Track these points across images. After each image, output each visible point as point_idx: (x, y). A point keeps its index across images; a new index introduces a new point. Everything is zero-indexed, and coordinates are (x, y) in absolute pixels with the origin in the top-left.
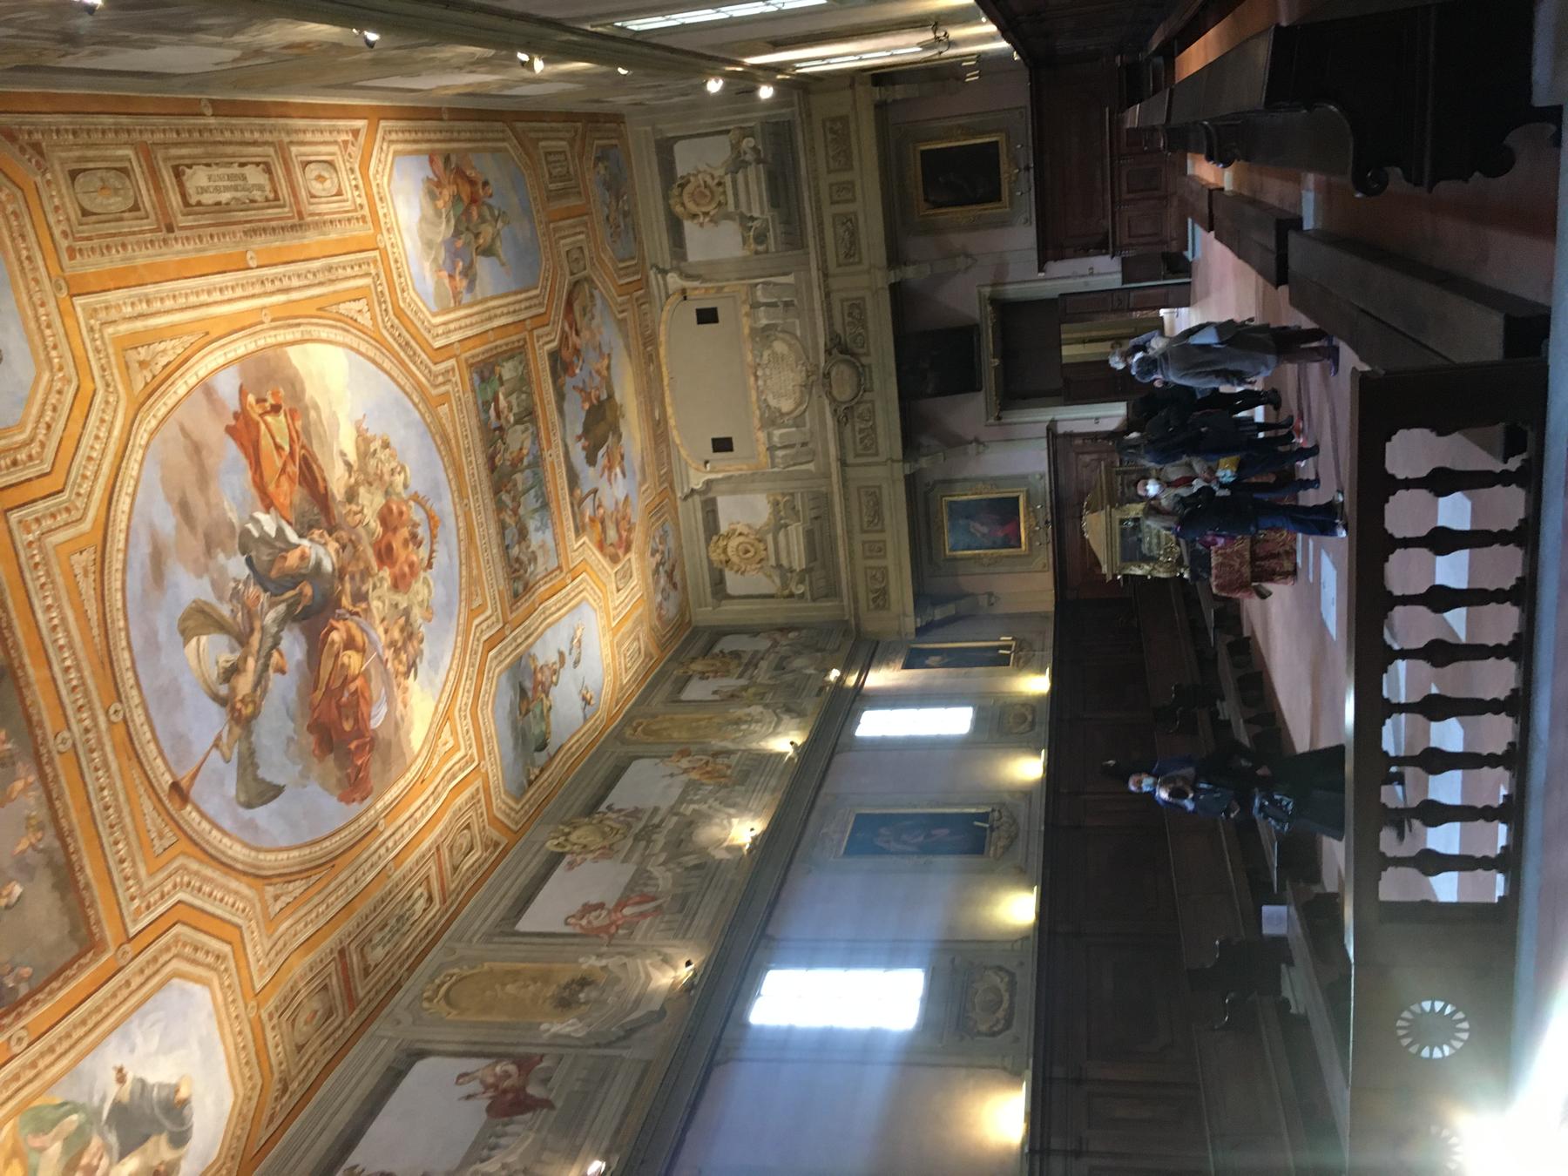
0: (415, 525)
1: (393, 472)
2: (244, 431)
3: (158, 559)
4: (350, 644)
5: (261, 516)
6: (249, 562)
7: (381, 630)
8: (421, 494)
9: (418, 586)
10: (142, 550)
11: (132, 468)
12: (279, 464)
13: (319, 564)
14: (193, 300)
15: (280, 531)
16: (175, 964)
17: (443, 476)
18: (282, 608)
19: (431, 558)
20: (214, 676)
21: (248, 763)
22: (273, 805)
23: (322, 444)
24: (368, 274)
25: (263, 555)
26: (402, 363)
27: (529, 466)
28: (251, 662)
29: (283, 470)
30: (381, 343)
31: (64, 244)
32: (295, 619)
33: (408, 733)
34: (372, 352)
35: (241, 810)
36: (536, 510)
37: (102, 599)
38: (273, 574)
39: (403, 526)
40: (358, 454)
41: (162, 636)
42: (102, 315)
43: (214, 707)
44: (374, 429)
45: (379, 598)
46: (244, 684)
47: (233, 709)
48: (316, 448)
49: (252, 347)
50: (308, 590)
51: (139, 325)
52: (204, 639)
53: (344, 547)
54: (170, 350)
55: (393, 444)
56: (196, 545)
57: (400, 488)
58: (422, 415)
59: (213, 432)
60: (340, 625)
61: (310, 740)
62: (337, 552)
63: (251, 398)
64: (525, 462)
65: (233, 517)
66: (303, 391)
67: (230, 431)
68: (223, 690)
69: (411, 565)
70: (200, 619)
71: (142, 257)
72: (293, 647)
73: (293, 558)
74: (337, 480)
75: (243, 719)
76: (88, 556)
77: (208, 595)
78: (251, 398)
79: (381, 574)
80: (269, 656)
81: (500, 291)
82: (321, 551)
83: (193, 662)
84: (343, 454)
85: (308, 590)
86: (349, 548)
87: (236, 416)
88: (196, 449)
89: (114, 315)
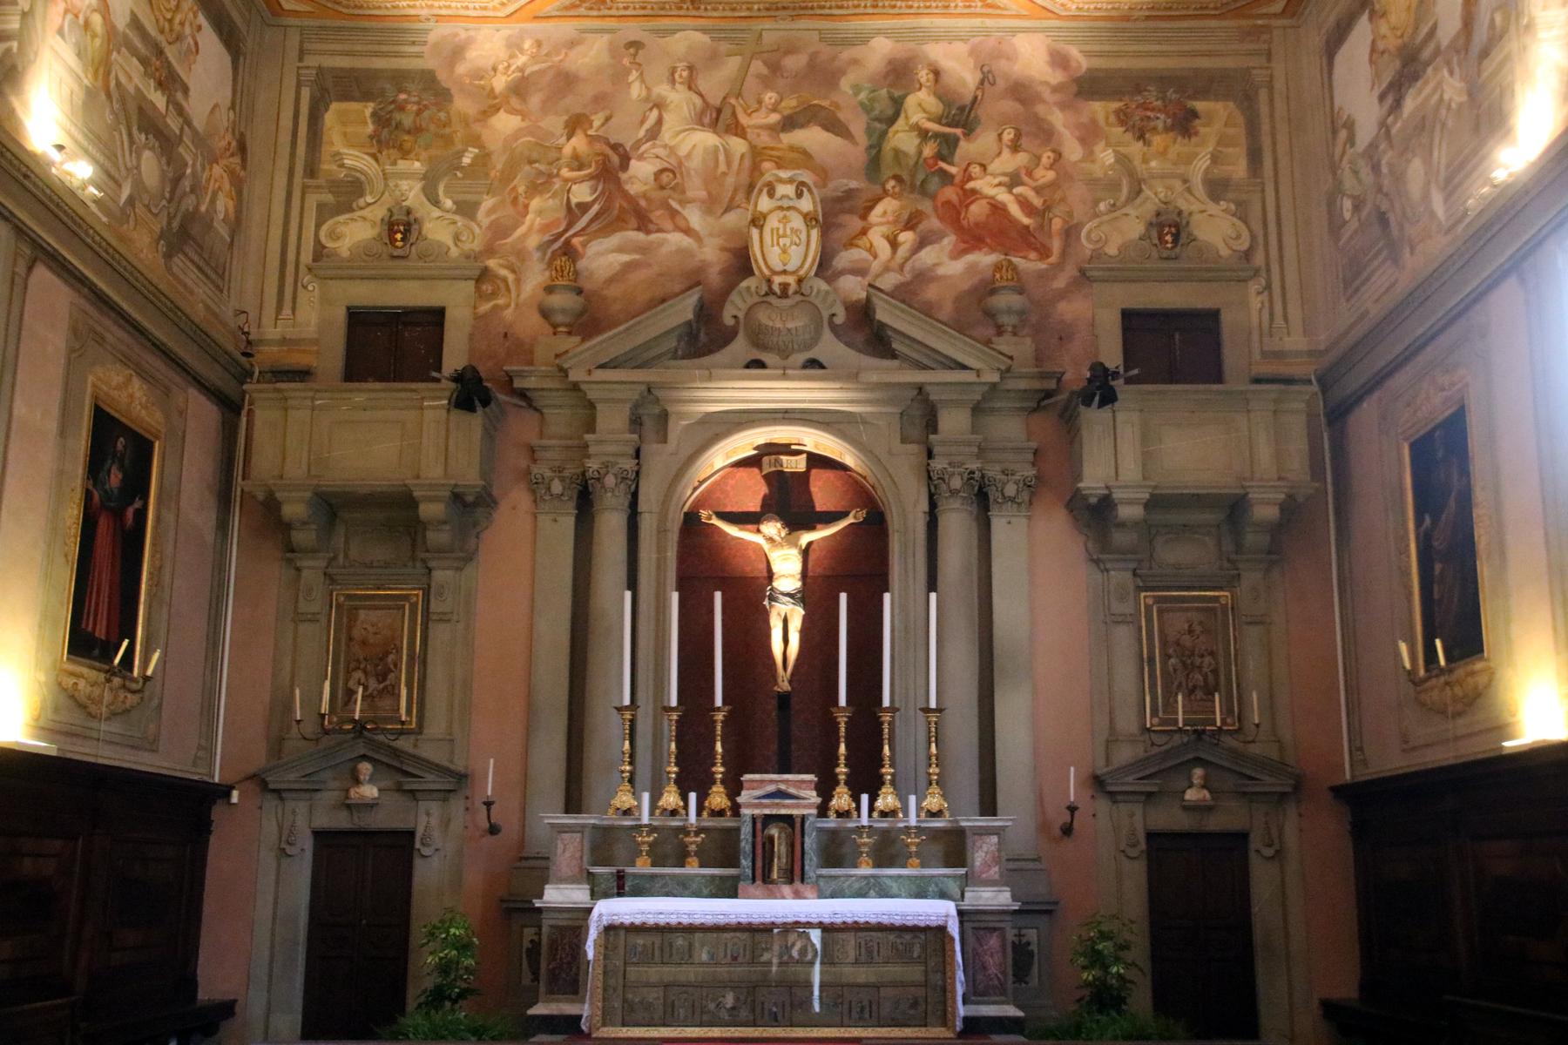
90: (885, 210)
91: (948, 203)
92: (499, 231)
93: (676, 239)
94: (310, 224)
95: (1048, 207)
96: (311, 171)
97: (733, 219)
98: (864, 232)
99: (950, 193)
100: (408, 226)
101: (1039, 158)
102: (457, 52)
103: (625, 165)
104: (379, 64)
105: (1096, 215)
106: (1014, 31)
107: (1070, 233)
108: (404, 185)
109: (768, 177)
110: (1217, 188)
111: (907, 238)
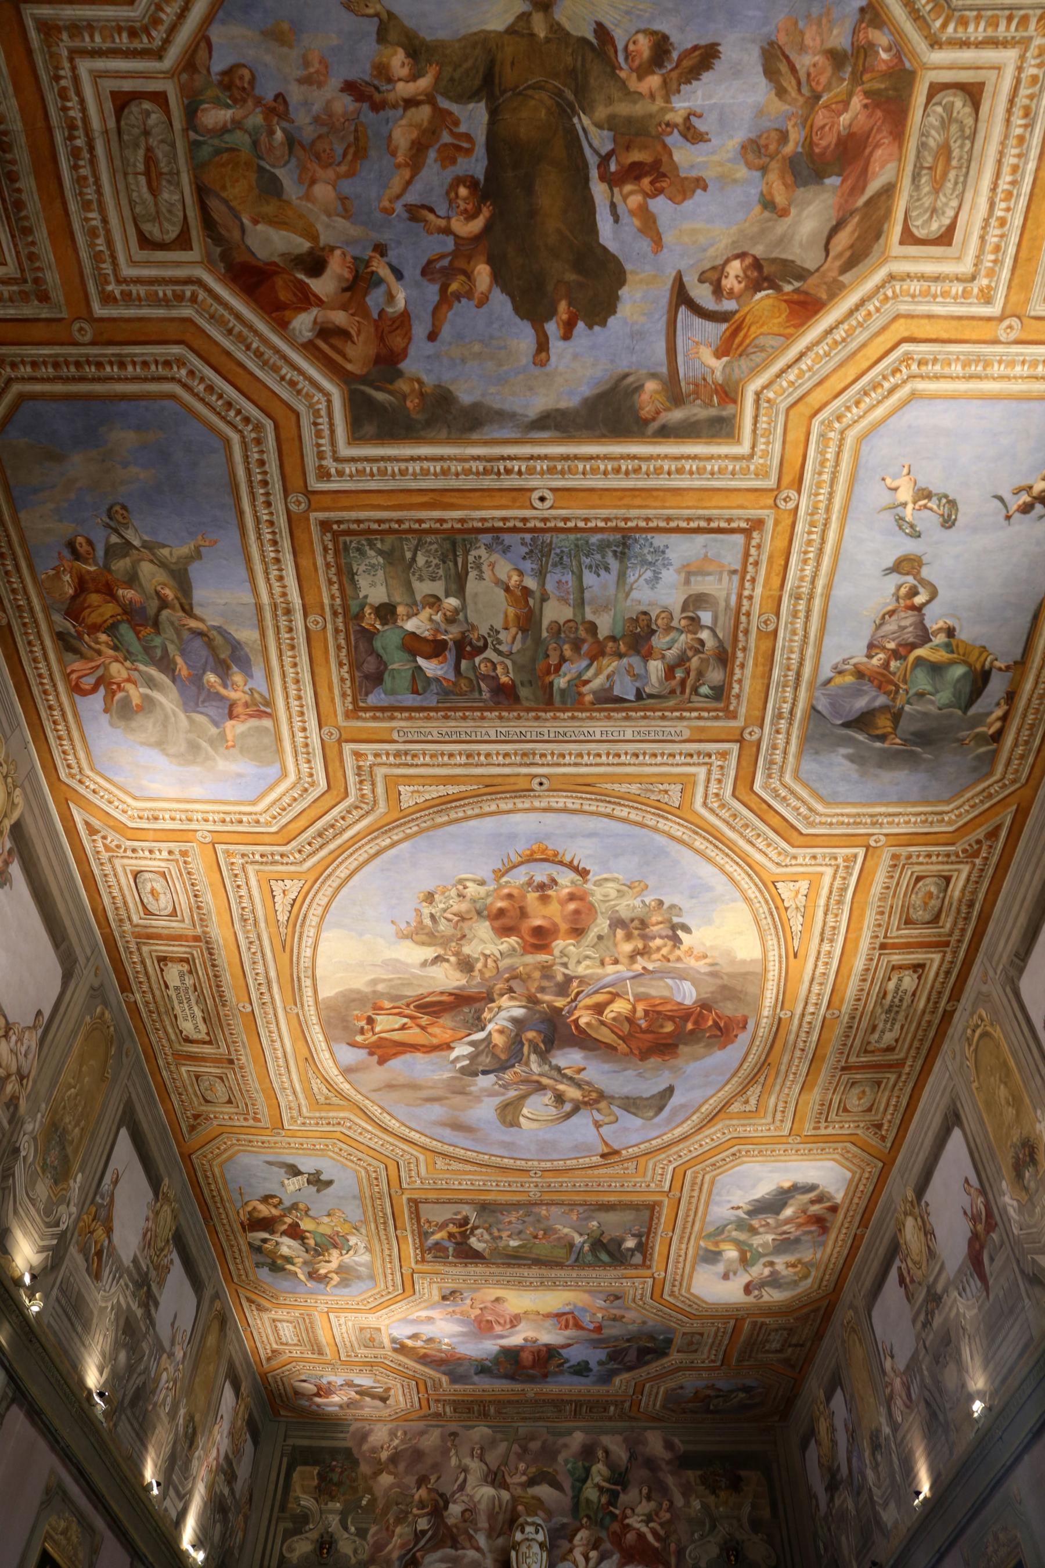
0: (529, 883)
1: (461, 896)
2: (384, 1051)
3: (458, 1126)
4: (599, 1009)
5: (454, 1055)
6: (485, 1073)
7: (610, 969)
8: (500, 866)
9: (597, 894)
10: (447, 1133)
11: (393, 1124)
12: (417, 1030)
13: (515, 1021)
14: (281, 1062)
15: (472, 1044)
16: (707, 1177)
17: (488, 823)
18: (533, 1057)
19: (576, 870)
20: (553, 1111)
21: (632, 1105)
22: (676, 1093)
23: (410, 984)
24: (244, 869)
25: (486, 1060)
26: (342, 849)
27: (541, 575)
28: (561, 1087)
29: (423, 1028)
30: (320, 874)
31: (251, 1122)
32: (548, 1051)
33: (733, 961)
34: (327, 891)
35: (656, 1120)
36: (622, 575)
37: (467, 1161)
38: (503, 1057)
39: (524, 897)
40: (430, 945)
41: (507, 1138)
42: (295, 1113)
43: (574, 1119)
44: (407, 916)
45: (579, 962)
46: (573, 1093)
47: (586, 1103)
48: (410, 993)
49: (317, 1028)
50: (531, 1035)
51: (301, 1095)
52: (525, 1111)
53: (511, 990)
54: (316, 1085)
55: (430, 887)
56: (458, 1099)
57: (482, 890)
58: (408, 837)
59: (380, 1074)
60: (577, 1014)
61: (654, 1061)
62: (512, 998)
63: (359, 1038)
64: (531, 583)
65: (447, 1075)
66: (359, 992)
67: (382, 1062)
68: (568, 1107)
69: (572, 897)
70: (509, 1114)
71: (254, 1083)
72: (569, 1059)
73: (498, 1040)
74: (447, 978)
75: (595, 1099)
76: (440, 1163)
77: (497, 1100)
78: (359, 1038)
79: (556, 952)
80: (565, 1076)
81: (244, 574)
82: (503, 1014)
83: (534, 1125)
84: (424, 964)
85: (531, 1035)
86: (514, 984)
87: (371, 1054)
88: (390, 1087)
89: (294, 1105)
90: (582, 1535)
91: (615, 1533)
92: (379, 1547)
93: (471, 1554)
94: (279, 1541)
95: (668, 1536)
96: (283, 1508)
97: (500, 1541)
98: (571, 1551)
99: (616, 1527)
100: (330, 1544)
101: (660, 1505)
102: (364, 1437)
103: (446, 1507)
104: (324, 1443)
105: (693, 1541)
106: (646, 1429)
107: (680, 1553)
108: (331, 1517)
109: (521, 1520)
110: (756, 1525)
111: (593, 1554)
